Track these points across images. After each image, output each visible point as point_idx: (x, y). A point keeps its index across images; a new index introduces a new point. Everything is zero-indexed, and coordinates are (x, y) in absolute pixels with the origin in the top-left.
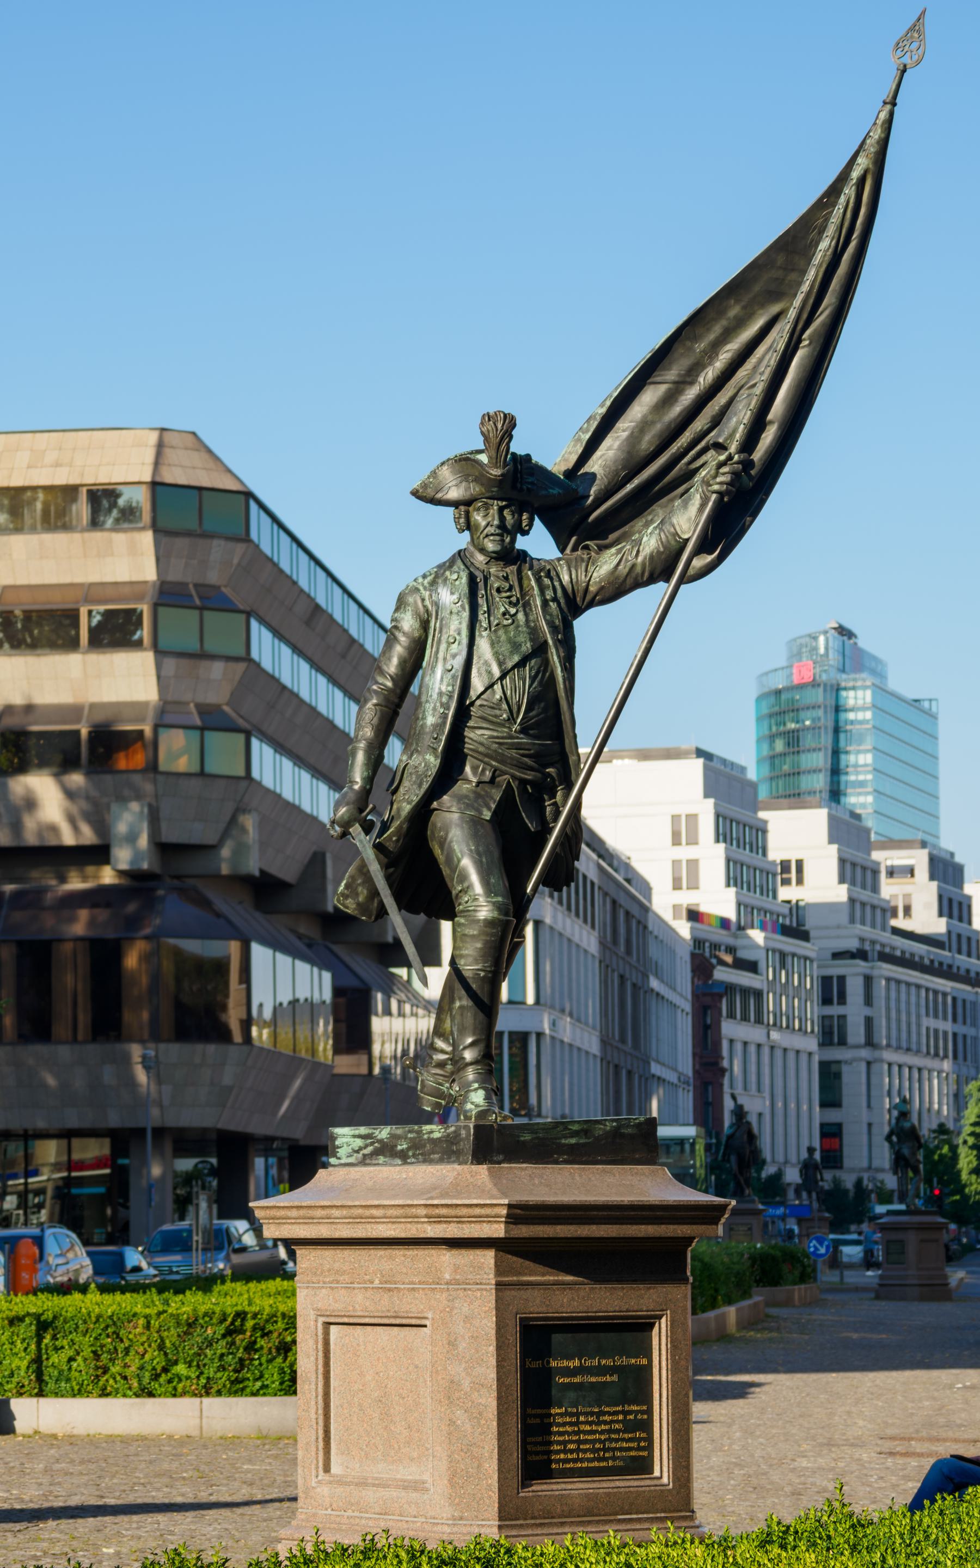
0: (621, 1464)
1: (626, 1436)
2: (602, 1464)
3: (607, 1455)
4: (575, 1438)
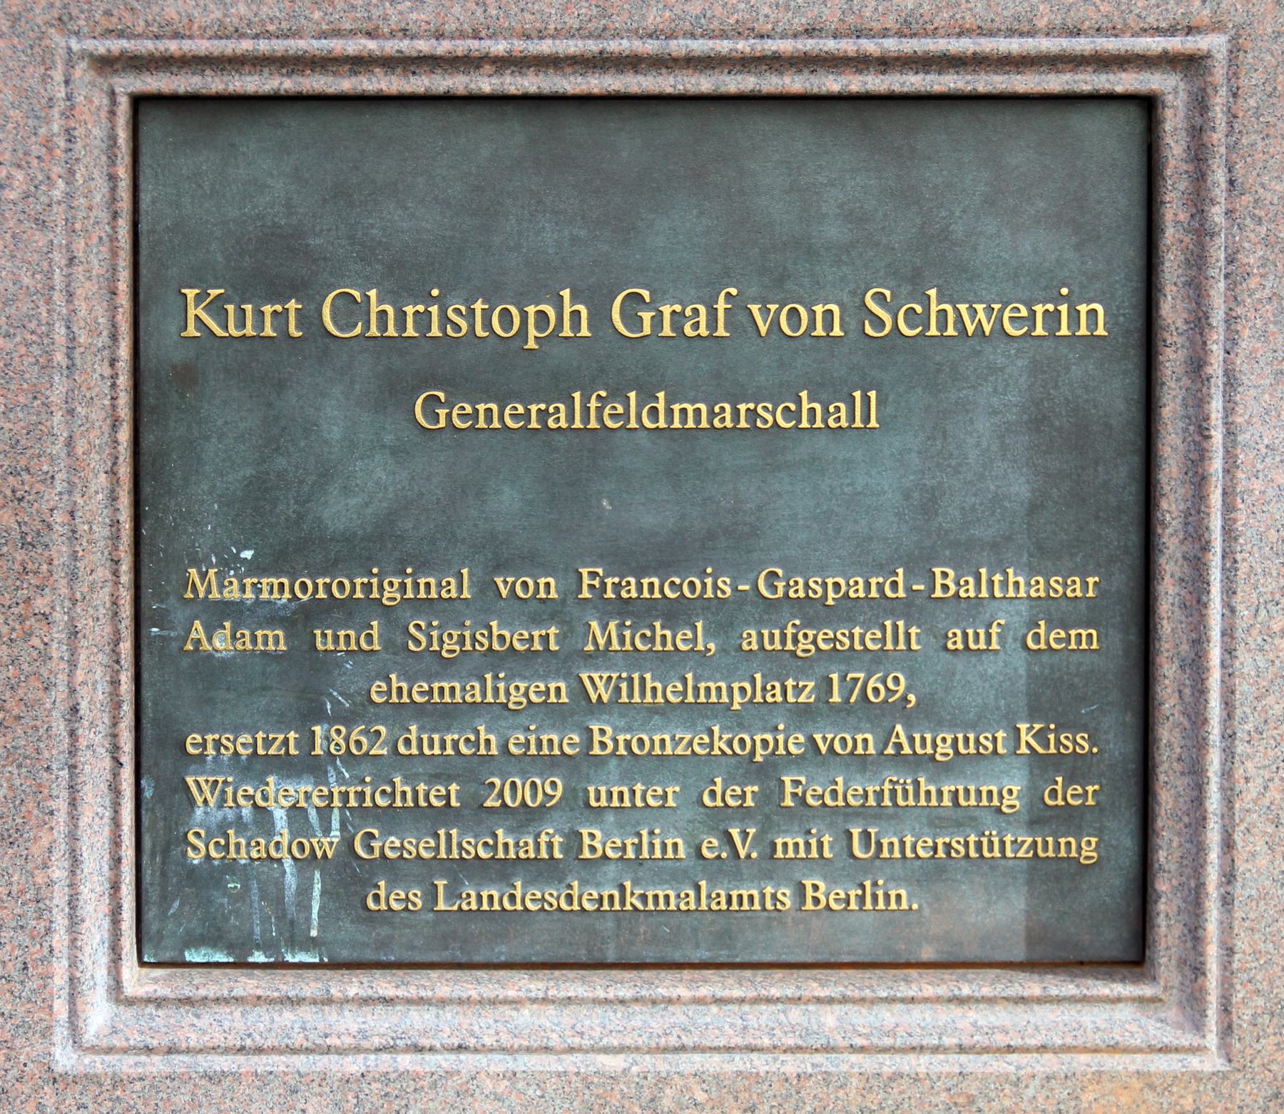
3: (788, 842)
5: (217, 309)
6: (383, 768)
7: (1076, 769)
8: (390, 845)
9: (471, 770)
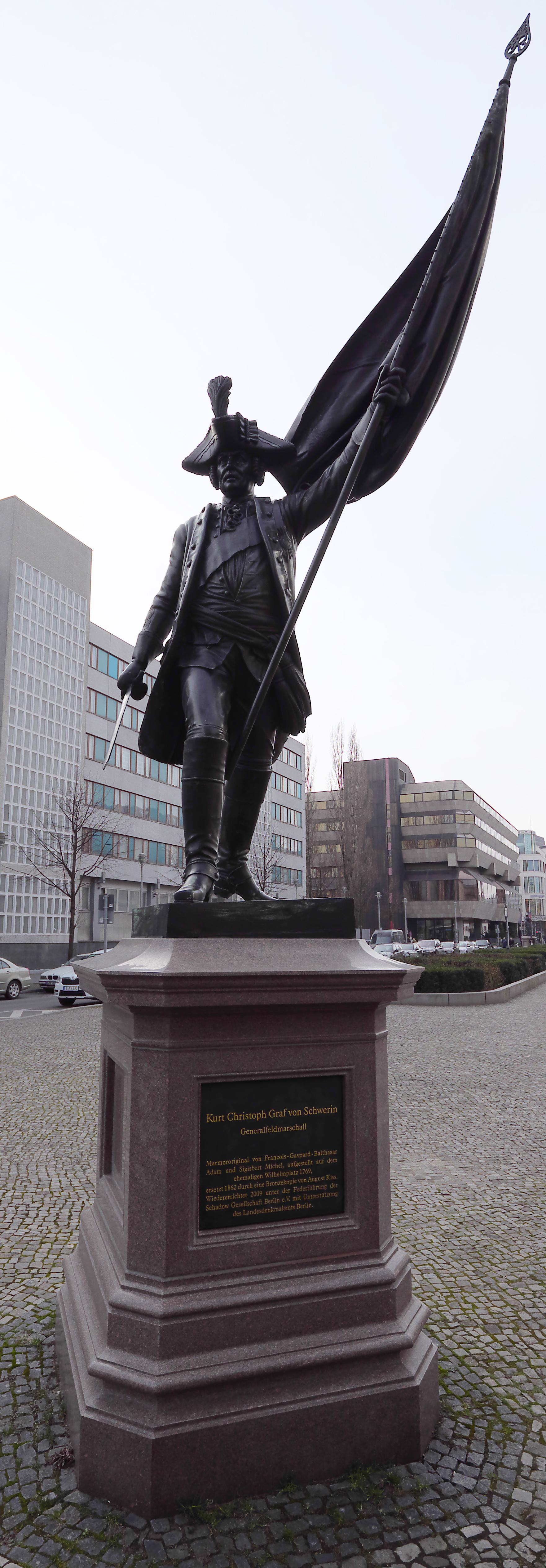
0: (310, 1206)
1: (316, 1180)
2: (288, 1208)
3: (294, 1199)
4: (262, 1185)
5: (212, 1118)
6: (235, 1192)
7: (334, 1181)
8: (236, 1205)
9: (248, 1191)
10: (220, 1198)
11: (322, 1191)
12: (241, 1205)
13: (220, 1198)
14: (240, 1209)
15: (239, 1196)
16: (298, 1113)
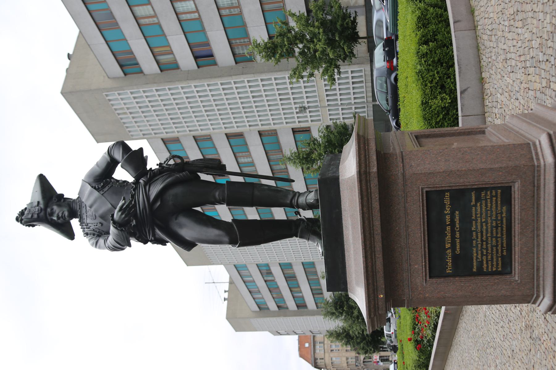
2: (504, 221)
3: (499, 218)
6: (492, 254)
7: (491, 193)
8: (500, 253)
10: (495, 263)
11: (496, 201)
12: (500, 251)
13: (495, 263)
14: (502, 252)
15: (494, 252)
16: (448, 218)
